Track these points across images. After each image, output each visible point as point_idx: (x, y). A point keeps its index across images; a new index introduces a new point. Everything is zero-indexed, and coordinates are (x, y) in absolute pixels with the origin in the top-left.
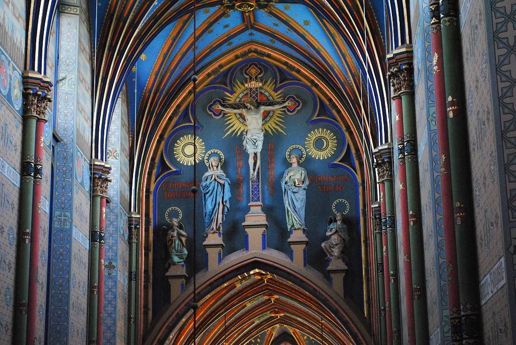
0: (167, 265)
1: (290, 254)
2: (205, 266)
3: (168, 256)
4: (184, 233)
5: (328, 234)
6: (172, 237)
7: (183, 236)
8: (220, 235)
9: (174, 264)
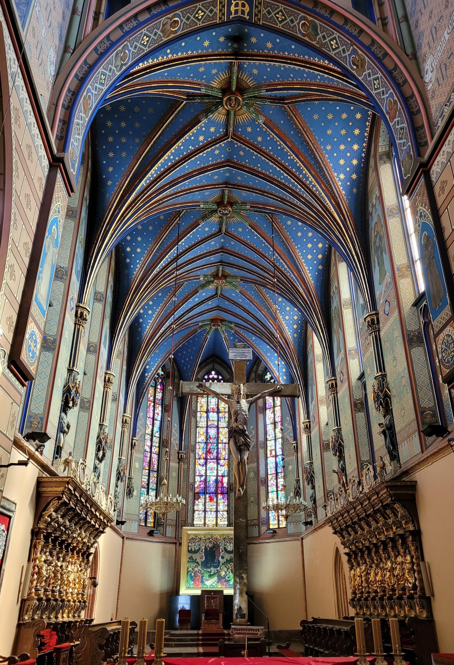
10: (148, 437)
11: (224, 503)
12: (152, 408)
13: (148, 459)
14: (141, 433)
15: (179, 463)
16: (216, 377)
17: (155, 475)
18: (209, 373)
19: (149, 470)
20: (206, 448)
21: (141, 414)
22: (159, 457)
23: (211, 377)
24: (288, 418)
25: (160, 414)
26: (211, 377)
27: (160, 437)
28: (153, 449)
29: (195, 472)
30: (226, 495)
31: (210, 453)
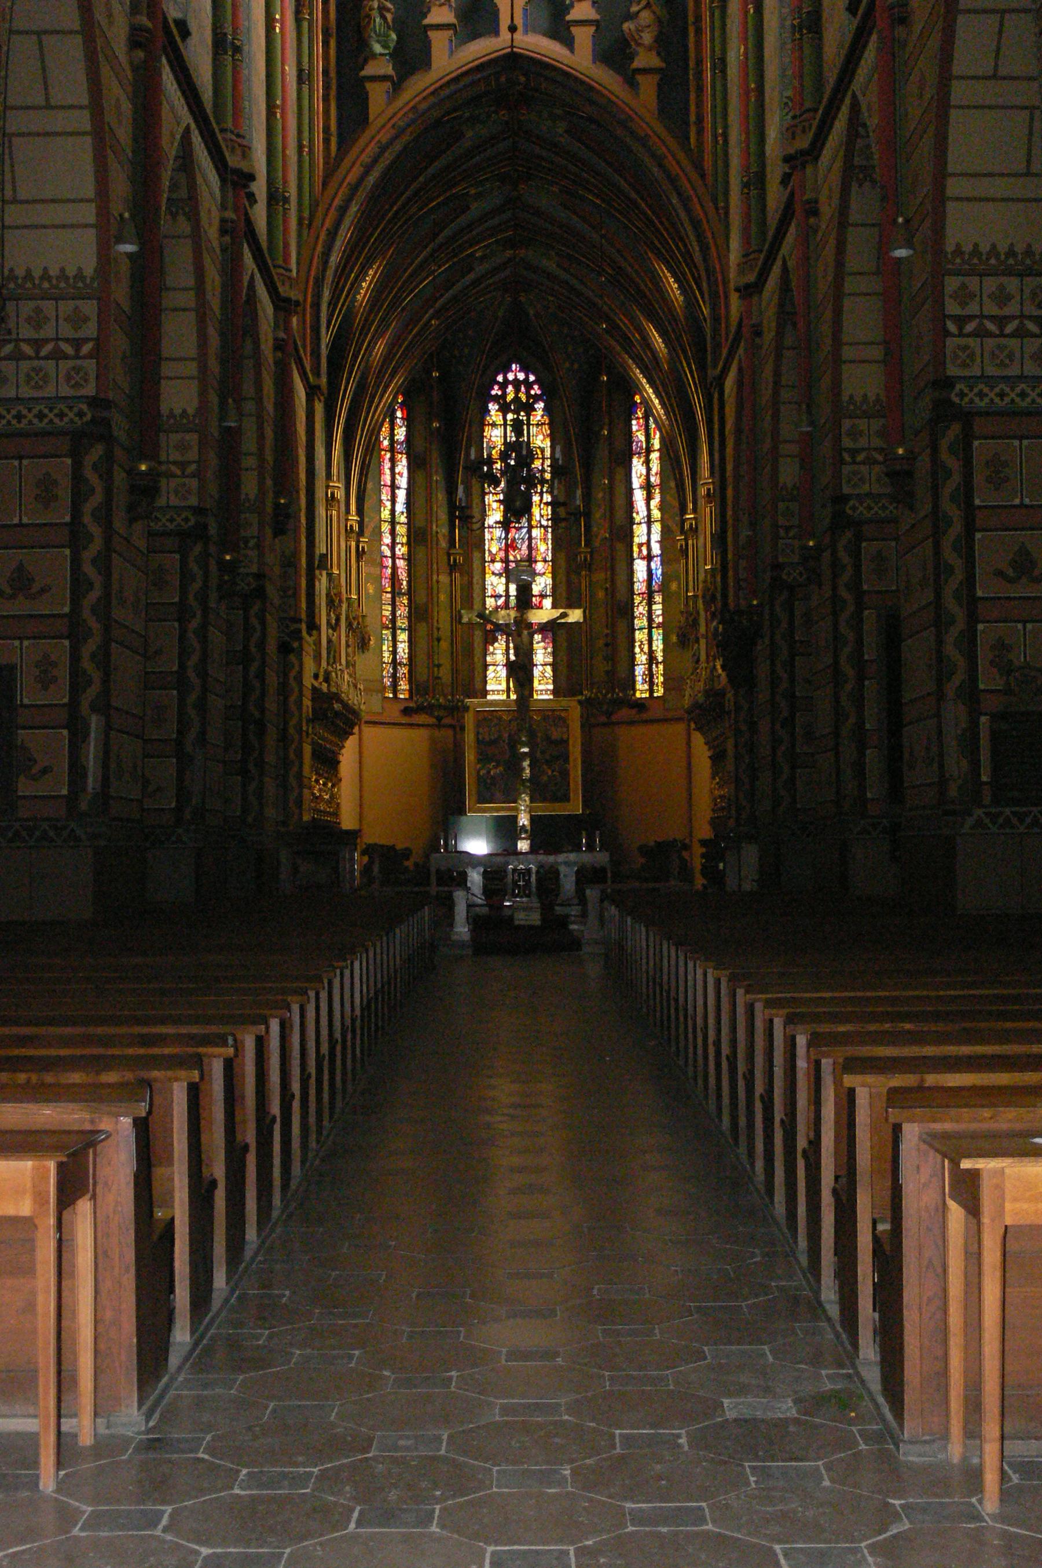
0: (361, 60)
1: (569, 42)
2: (425, 62)
3: (363, 44)
4: (389, 5)
5: (634, 9)
6: (372, 9)
7: (388, 10)
8: (450, 6)
9: (374, 56)
10: (386, 527)
11: (545, 649)
12: (387, 465)
13: (389, 571)
14: (372, 525)
15: (451, 574)
16: (521, 376)
17: (406, 602)
18: (507, 369)
19: (393, 592)
20: (506, 538)
21: (370, 486)
22: (409, 565)
23: (511, 376)
24: (673, 484)
25: (405, 474)
26: (511, 376)
27: (409, 524)
28: (397, 549)
29: (484, 589)
30: (550, 635)
31: (515, 549)
